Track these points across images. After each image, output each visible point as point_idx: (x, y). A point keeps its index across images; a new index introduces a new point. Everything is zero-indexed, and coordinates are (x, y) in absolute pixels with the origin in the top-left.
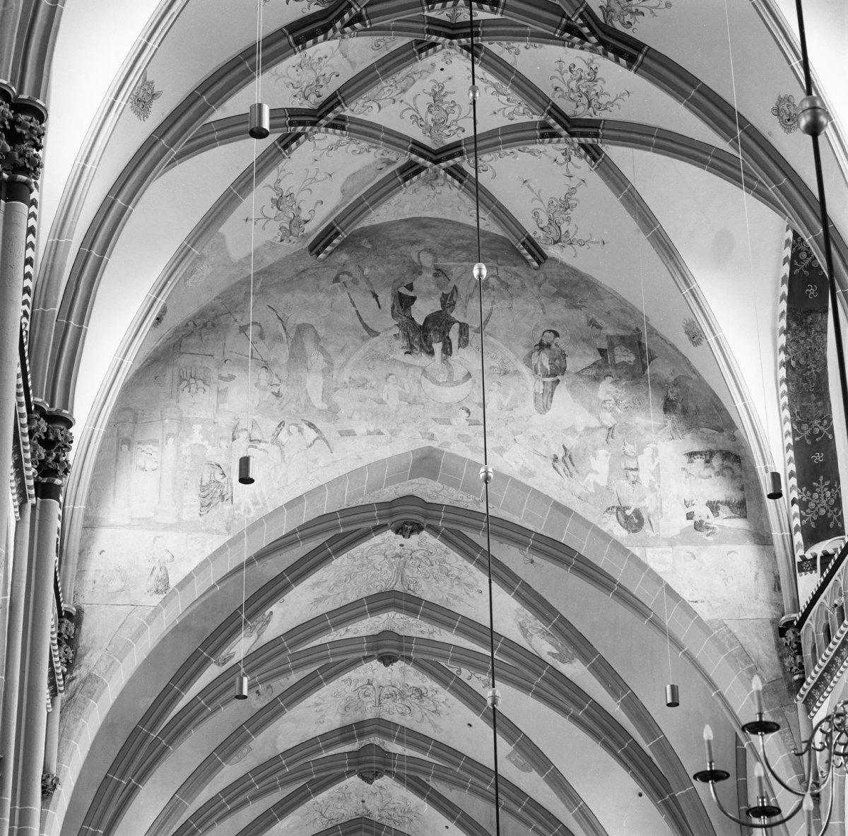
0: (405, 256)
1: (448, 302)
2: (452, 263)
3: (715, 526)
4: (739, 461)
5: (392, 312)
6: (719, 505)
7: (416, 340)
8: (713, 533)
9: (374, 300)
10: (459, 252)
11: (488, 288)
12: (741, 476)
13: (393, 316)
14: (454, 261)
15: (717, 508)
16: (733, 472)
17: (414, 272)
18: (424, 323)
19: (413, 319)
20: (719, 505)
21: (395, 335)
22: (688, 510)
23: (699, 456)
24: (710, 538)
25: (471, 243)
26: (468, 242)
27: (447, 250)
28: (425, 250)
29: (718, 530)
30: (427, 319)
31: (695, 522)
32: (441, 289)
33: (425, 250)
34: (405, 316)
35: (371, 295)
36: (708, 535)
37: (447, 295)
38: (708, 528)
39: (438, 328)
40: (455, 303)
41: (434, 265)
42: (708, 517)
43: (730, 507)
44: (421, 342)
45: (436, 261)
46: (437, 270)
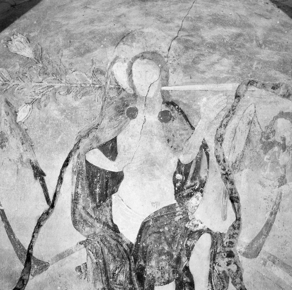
0: (102, 73)
1: (189, 183)
2: (199, 87)
5: (74, 213)
7: (122, 278)
9: (37, 184)
10: (215, 57)
11: (272, 145)
13: (75, 223)
14: (204, 81)
17: (119, 111)
18: (137, 242)
19: (115, 229)
21: (79, 269)
25: (239, 35)
26: (234, 31)
27: (193, 53)
28: (142, 56)
30: (144, 227)
32: (175, 149)
33: (142, 56)
34: (98, 220)
35: (30, 173)
37: (188, 166)
39: (166, 248)
40: (203, 184)
41: (163, 92)
44: (131, 282)
45: (165, 81)
46: (168, 104)
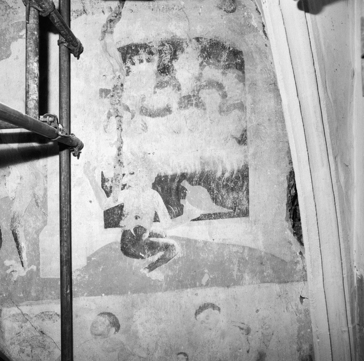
3: (171, 242)
4: (241, 67)
6: (185, 184)
8: (163, 260)
12: (242, 107)
15: (180, 193)
16: (224, 96)
20: (185, 184)
22: (110, 203)
23: (144, 55)
24: (157, 275)
29: (179, 251)
31: (125, 233)
36: (152, 267)
38: (153, 247)
42: (156, 219)
43: (210, 190)
